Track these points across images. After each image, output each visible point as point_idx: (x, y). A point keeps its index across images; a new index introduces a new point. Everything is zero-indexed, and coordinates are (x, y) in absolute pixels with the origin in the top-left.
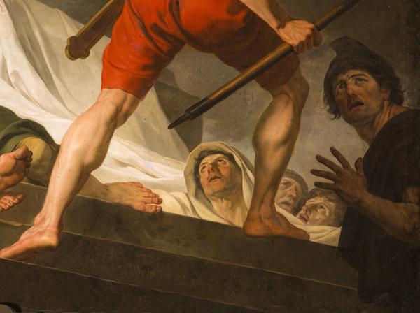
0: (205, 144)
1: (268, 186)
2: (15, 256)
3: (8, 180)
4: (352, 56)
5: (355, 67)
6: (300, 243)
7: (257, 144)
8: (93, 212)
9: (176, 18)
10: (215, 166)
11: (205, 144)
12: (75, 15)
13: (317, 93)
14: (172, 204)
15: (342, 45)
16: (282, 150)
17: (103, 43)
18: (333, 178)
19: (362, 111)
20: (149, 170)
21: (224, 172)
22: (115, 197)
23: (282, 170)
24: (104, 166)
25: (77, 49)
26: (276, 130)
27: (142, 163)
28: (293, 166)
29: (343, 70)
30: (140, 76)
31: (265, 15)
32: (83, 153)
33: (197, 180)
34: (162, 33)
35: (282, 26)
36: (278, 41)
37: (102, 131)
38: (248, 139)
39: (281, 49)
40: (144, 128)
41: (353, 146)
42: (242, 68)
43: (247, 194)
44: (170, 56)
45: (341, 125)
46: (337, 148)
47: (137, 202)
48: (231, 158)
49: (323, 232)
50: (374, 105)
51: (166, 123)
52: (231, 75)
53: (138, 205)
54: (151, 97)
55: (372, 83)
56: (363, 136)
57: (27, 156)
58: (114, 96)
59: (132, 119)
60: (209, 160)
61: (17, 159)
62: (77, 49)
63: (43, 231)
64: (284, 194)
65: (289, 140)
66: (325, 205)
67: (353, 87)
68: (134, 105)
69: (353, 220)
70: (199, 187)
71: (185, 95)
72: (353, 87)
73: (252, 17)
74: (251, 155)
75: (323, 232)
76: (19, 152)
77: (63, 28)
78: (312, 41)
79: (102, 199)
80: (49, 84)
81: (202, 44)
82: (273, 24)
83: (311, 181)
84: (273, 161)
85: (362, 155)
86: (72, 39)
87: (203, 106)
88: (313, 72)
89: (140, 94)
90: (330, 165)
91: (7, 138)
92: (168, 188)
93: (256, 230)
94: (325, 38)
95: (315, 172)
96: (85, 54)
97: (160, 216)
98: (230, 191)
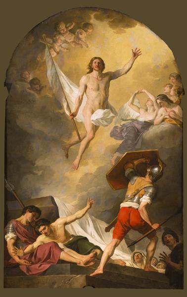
0: (136, 251)
1: (149, 260)
2: (94, 275)
3: (92, 259)
4: (168, 231)
5: (169, 234)
6: (156, 273)
7: (147, 251)
8: (111, 266)
9: (129, 223)
10: (138, 256)
11: (135, 251)
12: (107, 222)
13: (160, 240)
14: (128, 264)
15: (166, 229)
16: (152, 253)
17: (113, 228)
18: (164, 258)
19: (170, 244)
20: (123, 257)
21: (140, 257)
22: (115, 263)
23: (152, 257)
24: (113, 256)
25: (107, 230)
26: (151, 248)
27: (121, 255)
28: (154, 256)
29: (166, 235)
30: (121, 236)
31: (149, 222)
32: (108, 253)
33: (134, 260)
34: (126, 226)
35: (152, 225)
36: (152, 228)
37: (113, 248)
38: (145, 250)
39: (152, 230)
40: (122, 247)
41: (168, 251)
42: (144, 234)
43: (145, 262)
44: (128, 231)
45: (165, 246)
46: (165, 252)
48: (141, 254)
49: (161, 270)
50: (173, 242)
51: (127, 246)
52: (141, 236)
53: (121, 264)
54: (124, 240)
55: (172, 237)
56: (170, 249)
57: (96, 253)
58: (115, 240)
59: (119, 245)
60: (136, 254)
61: (94, 254)
62: (107, 230)
63: (100, 270)
64: (153, 262)
65: (154, 250)
66: (162, 264)
67: (168, 238)
68: (120, 242)
69: (168, 268)
70: (134, 260)
71: (131, 240)
72: (168, 238)
73: (146, 223)
74: (145, 253)
75: (161, 270)
76: (95, 252)
77: (104, 225)
78: (159, 228)
79: (112, 263)
80: (101, 238)
81: (135, 229)
82: (150, 224)
83: (159, 259)
84: (150, 254)
85: (170, 253)
86: (106, 228)
87: (135, 242)
88: (159, 235)
89: (121, 240)
90: (163, 255)
91: (92, 249)
92: (127, 261)
93: (147, 270)
94: (162, 227)
95: (159, 257)
96: (109, 231)
97: (126, 266)
98: (141, 261)
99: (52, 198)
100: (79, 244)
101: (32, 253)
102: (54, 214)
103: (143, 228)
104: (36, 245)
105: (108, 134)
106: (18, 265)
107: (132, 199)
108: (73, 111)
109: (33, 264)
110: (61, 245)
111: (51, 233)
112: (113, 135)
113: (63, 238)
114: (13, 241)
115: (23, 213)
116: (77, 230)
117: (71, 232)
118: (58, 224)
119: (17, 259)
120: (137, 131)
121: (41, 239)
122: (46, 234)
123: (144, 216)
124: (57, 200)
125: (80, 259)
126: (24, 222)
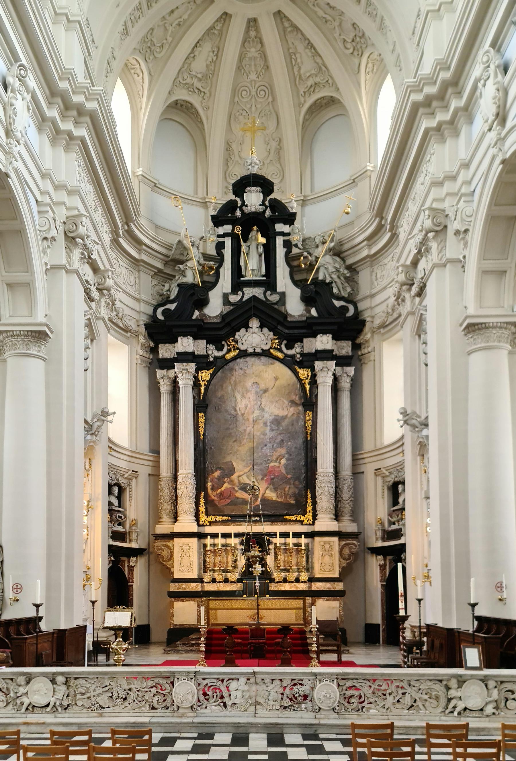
6: (290, 503)
8: (264, 500)
14: (274, 499)
18: (294, 495)
20: (271, 495)
25: (262, 479)
26: (287, 489)
47: (270, 498)
49: (293, 502)
64: (288, 496)
69: (296, 500)
84: (287, 493)
98: (281, 497)
99: (231, 462)
101: (221, 494)
102: (232, 471)
104: (223, 489)
105: (262, 425)
106: (213, 500)
107: (276, 461)
108: (243, 412)
109: (221, 499)
110: (236, 489)
111: (231, 482)
113: (237, 484)
114: (211, 487)
115: (216, 471)
116: (245, 480)
117: (242, 481)
118: (234, 477)
119: (213, 498)
120: (277, 421)
121: (226, 485)
122: (228, 482)
123: (284, 471)
124: (234, 463)
126: (216, 476)
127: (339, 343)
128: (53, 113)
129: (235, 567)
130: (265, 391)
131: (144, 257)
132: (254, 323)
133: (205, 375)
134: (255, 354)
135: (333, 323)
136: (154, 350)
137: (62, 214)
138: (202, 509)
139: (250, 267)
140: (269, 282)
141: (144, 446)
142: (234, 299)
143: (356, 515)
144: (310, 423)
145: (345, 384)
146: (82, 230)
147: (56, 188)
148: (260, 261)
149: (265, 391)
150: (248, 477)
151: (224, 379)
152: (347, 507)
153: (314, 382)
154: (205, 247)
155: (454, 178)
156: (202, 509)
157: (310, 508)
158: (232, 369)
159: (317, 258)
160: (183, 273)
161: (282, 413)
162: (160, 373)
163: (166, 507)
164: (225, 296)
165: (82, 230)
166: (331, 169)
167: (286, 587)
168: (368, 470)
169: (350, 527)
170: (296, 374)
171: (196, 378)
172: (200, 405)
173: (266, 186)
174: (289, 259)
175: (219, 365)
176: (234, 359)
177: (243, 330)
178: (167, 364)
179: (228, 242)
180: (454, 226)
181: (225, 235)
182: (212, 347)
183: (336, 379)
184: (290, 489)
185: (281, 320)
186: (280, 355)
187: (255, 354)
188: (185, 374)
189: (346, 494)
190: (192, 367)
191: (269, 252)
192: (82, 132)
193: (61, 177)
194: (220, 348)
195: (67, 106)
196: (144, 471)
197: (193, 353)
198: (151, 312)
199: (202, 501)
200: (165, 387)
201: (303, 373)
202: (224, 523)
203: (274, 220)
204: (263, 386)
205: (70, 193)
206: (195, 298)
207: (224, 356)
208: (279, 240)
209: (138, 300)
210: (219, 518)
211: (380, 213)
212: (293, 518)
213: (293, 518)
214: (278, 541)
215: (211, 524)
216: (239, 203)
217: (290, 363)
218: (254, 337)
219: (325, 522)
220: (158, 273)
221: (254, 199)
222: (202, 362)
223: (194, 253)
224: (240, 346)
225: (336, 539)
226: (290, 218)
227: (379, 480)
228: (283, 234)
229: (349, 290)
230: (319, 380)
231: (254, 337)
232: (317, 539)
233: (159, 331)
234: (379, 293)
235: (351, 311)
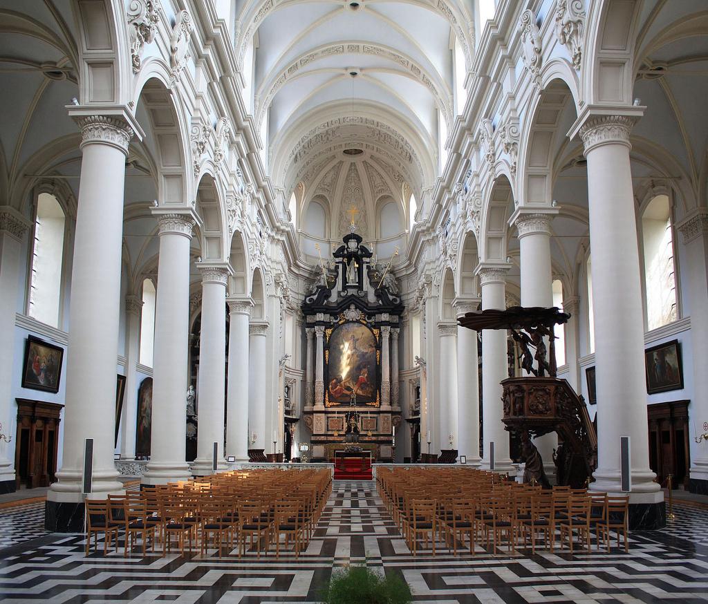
20: (360, 392)
77: (355, 383)
100: (348, 389)
103: (365, 383)
111: (341, 386)
112: (357, 356)
120: (363, 355)
125: (348, 393)
127: (393, 317)
128: (273, 234)
129: (343, 428)
130: (358, 340)
131: (301, 273)
132: (353, 307)
133: (329, 331)
134: (353, 322)
135: (390, 309)
136: (304, 318)
137: (274, 273)
138: (327, 399)
139: (351, 278)
140: (360, 287)
141: (299, 367)
142: (342, 294)
143: (400, 403)
144: (378, 356)
145: (395, 336)
146: (282, 280)
147: (272, 262)
148: (355, 275)
149: (358, 340)
150: (349, 383)
151: (338, 333)
152: (396, 398)
153: (380, 336)
154: (329, 266)
155: (438, 259)
156: (327, 399)
157: (378, 399)
158: (342, 329)
159: (382, 275)
160: (319, 281)
161: (365, 351)
162: (307, 330)
163: (309, 397)
164: (339, 292)
165: (282, 280)
166: (389, 230)
167: (367, 439)
168: (406, 380)
169: (398, 409)
170: (372, 331)
171: (324, 333)
172: (326, 347)
173: (359, 239)
174: (369, 276)
175: (336, 327)
176: (343, 324)
177: (347, 310)
178: (312, 325)
179: (341, 266)
180: (434, 283)
181: (339, 263)
182: (332, 318)
183: (391, 334)
184: (369, 389)
185: (365, 305)
186: (365, 322)
187: (353, 322)
188: (319, 331)
189: (395, 392)
190: (324, 327)
191: (360, 270)
192: (284, 238)
193: (274, 258)
194: (336, 319)
195: (278, 230)
196: (299, 379)
197: (323, 321)
198: (304, 299)
199: (327, 395)
200: (309, 337)
201: (376, 331)
202: (337, 406)
203: (363, 256)
204: (356, 337)
205: (277, 263)
206: (325, 294)
207: (338, 323)
208: (365, 266)
209: (298, 294)
210: (335, 404)
211: (410, 259)
212: (370, 404)
213: (370, 404)
214: (361, 415)
215: (331, 406)
216: (346, 247)
217: (371, 327)
218: (352, 314)
219: (385, 407)
220: (307, 279)
221: (353, 245)
222: (327, 325)
223: (325, 271)
224: (346, 317)
225: (390, 415)
226: (370, 255)
227: (411, 385)
228: (367, 263)
229: (397, 290)
230: (383, 335)
231: (352, 314)
232: (381, 415)
233: (307, 310)
234: (410, 298)
235: (398, 299)
